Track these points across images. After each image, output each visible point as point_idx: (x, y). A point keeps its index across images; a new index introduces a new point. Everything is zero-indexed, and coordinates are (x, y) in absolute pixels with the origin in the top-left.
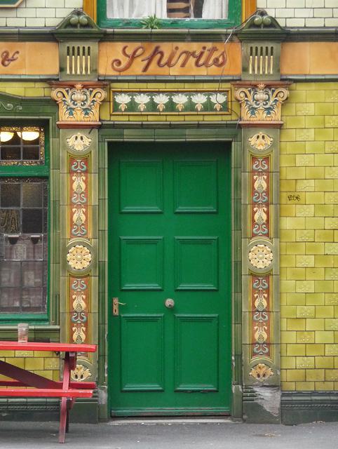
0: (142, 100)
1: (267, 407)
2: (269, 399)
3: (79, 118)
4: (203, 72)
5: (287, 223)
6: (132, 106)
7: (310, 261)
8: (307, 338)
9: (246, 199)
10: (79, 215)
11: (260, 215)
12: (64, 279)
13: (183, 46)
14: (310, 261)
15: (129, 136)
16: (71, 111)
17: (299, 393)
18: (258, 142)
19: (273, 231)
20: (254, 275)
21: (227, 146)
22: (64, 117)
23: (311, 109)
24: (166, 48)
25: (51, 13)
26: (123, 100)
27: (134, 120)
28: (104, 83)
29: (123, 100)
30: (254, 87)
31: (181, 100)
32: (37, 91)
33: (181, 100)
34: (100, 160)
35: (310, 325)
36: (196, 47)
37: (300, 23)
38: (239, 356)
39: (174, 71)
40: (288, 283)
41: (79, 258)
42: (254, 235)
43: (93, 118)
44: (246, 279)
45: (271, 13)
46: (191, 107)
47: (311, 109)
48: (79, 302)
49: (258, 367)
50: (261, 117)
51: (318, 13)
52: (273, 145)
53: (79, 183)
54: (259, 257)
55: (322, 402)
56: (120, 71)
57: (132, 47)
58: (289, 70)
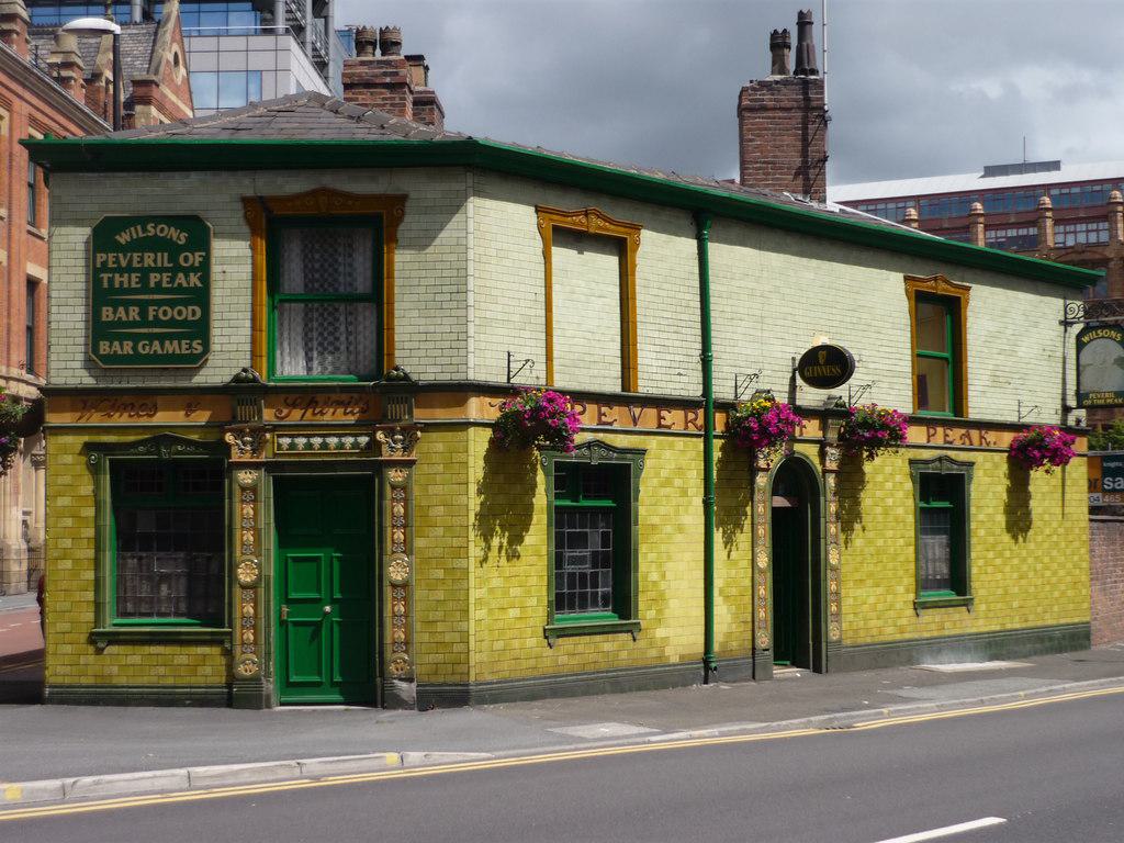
1: (404, 696)
2: (406, 690)
5: (419, 543)
7: (440, 574)
8: (439, 638)
9: (388, 522)
12: (237, 591)
14: (440, 574)
17: (433, 685)
18: (395, 476)
20: (394, 586)
21: (371, 479)
22: (235, 456)
25: (227, 371)
35: (440, 627)
37: (432, 377)
38: (382, 653)
40: (419, 593)
42: (393, 552)
44: (388, 591)
45: (408, 369)
49: (395, 662)
50: (398, 456)
51: (446, 368)
52: (409, 476)
54: (396, 572)
55: (451, 691)
56: (282, 418)
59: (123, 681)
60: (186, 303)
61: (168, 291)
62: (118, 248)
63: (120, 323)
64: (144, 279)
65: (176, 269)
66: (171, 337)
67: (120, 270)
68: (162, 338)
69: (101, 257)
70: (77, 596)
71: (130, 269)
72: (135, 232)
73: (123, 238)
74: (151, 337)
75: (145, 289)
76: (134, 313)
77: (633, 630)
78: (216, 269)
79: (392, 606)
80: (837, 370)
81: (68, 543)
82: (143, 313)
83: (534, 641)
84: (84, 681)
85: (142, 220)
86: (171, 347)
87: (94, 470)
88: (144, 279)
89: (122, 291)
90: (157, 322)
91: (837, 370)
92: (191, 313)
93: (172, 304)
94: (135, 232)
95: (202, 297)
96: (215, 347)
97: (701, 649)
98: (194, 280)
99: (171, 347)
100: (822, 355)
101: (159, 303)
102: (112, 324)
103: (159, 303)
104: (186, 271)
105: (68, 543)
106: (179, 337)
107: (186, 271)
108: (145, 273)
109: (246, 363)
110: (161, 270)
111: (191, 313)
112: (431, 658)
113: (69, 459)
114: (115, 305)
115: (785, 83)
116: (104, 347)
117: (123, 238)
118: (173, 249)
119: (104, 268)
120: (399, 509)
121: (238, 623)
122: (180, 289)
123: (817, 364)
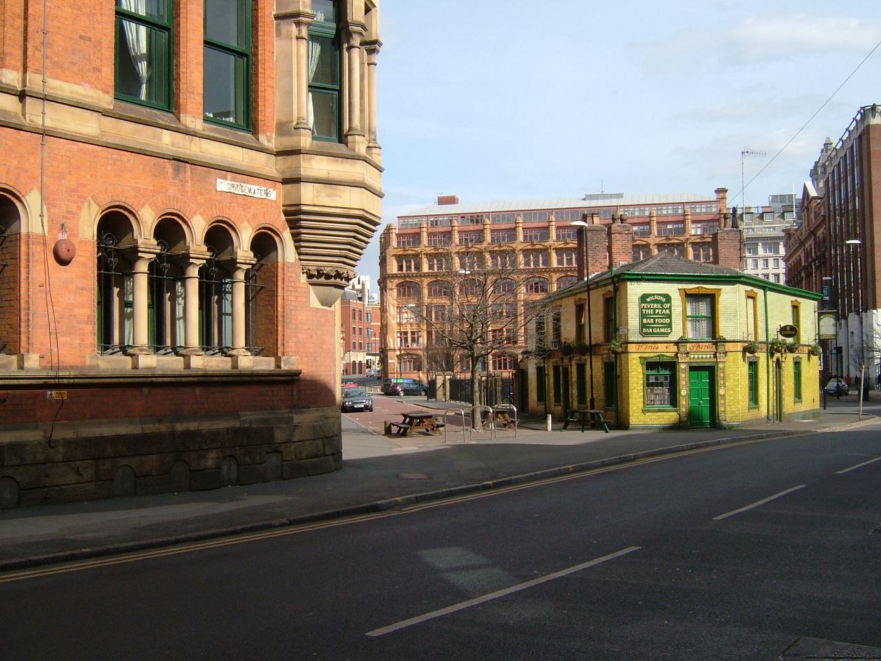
0: (696, 356)
3: (683, 361)
4: (709, 350)
5: (727, 384)
6: (694, 358)
7: (732, 392)
9: (719, 378)
10: (684, 383)
11: (722, 382)
13: (704, 344)
15: (694, 365)
16: (682, 359)
18: (721, 366)
19: (724, 385)
22: (680, 361)
23: (731, 358)
24: (701, 344)
26: (692, 356)
27: (695, 361)
28: (688, 353)
29: (692, 356)
30: (720, 353)
31: (704, 356)
32: (673, 355)
33: (704, 356)
34: (688, 370)
35: (732, 407)
36: (707, 344)
39: (703, 350)
40: (727, 397)
41: (684, 392)
43: (687, 360)
44: (719, 397)
46: (706, 358)
47: (731, 358)
48: (684, 403)
50: (722, 360)
53: (683, 375)
54: (721, 392)
57: (693, 344)
58: (726, 350)
59: (651, 423)
60: (666, 318)
61: (662, 315)
62: (647, 302)
63: (648, 324)
64: (654, 311)
65: (663, 309)
66: (662, 327)
67: (648, 309)
68: (660, 328)
69: (643, 305)
70: (638, 400)
71: (650, 308)
72: (652, 298)
73: (648, 300)
74: (657, 327)
75: (654, 314)
76: (652, 320)
77: (758, 408)
78: (672, 308)
79: (721, 402)
80: (794, 333)
81: (635, 385)
82: (654, 321)
83: (747, 411)
84: (640, 423)
85: (654, 295)
86: (662, 330)
87: (642, 364)
88: (654, 311)
89: (648, 314)
90: (658, 324)
91: (794, 333)
92: (667, 321)
93: (662, 318)
94: (652, 298)
95: (669, 316)
96: (673, 330)
97: (766, 414)
98: (668, 311)
99: (662, 330)
100: (788, 328)
101: (659, 318)
102: (646, 324)
103: (659, 318)
104: (666, 309)
105: (635, 385)
106: (664, 327)
107: (666, 309)
108: (655, 309)
109: (682, 335)
110: (659, 309)
111: (667, 321)
112: (730, 415)
113: (635, 361)
114: (647, 318)
115: (731, 231)
116: (644, 330)
117: (648, 300)
118: (662, 304)
119: (644, 308)
120: (722, 375)
121: (681, 407)
122: (664, 314)
123: (786, 330)
